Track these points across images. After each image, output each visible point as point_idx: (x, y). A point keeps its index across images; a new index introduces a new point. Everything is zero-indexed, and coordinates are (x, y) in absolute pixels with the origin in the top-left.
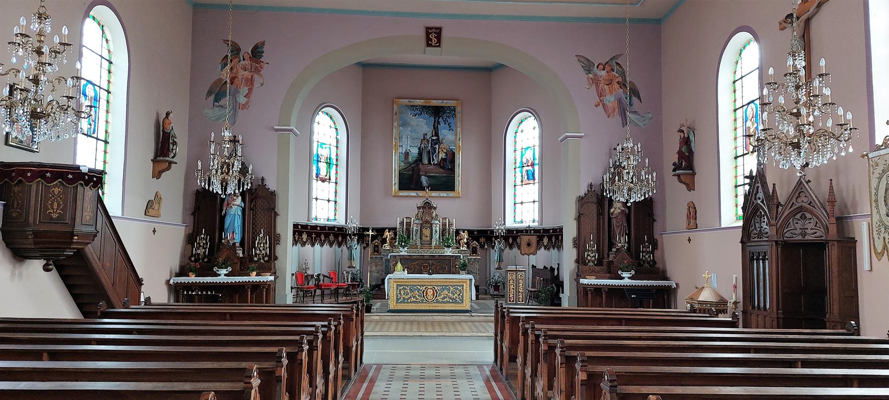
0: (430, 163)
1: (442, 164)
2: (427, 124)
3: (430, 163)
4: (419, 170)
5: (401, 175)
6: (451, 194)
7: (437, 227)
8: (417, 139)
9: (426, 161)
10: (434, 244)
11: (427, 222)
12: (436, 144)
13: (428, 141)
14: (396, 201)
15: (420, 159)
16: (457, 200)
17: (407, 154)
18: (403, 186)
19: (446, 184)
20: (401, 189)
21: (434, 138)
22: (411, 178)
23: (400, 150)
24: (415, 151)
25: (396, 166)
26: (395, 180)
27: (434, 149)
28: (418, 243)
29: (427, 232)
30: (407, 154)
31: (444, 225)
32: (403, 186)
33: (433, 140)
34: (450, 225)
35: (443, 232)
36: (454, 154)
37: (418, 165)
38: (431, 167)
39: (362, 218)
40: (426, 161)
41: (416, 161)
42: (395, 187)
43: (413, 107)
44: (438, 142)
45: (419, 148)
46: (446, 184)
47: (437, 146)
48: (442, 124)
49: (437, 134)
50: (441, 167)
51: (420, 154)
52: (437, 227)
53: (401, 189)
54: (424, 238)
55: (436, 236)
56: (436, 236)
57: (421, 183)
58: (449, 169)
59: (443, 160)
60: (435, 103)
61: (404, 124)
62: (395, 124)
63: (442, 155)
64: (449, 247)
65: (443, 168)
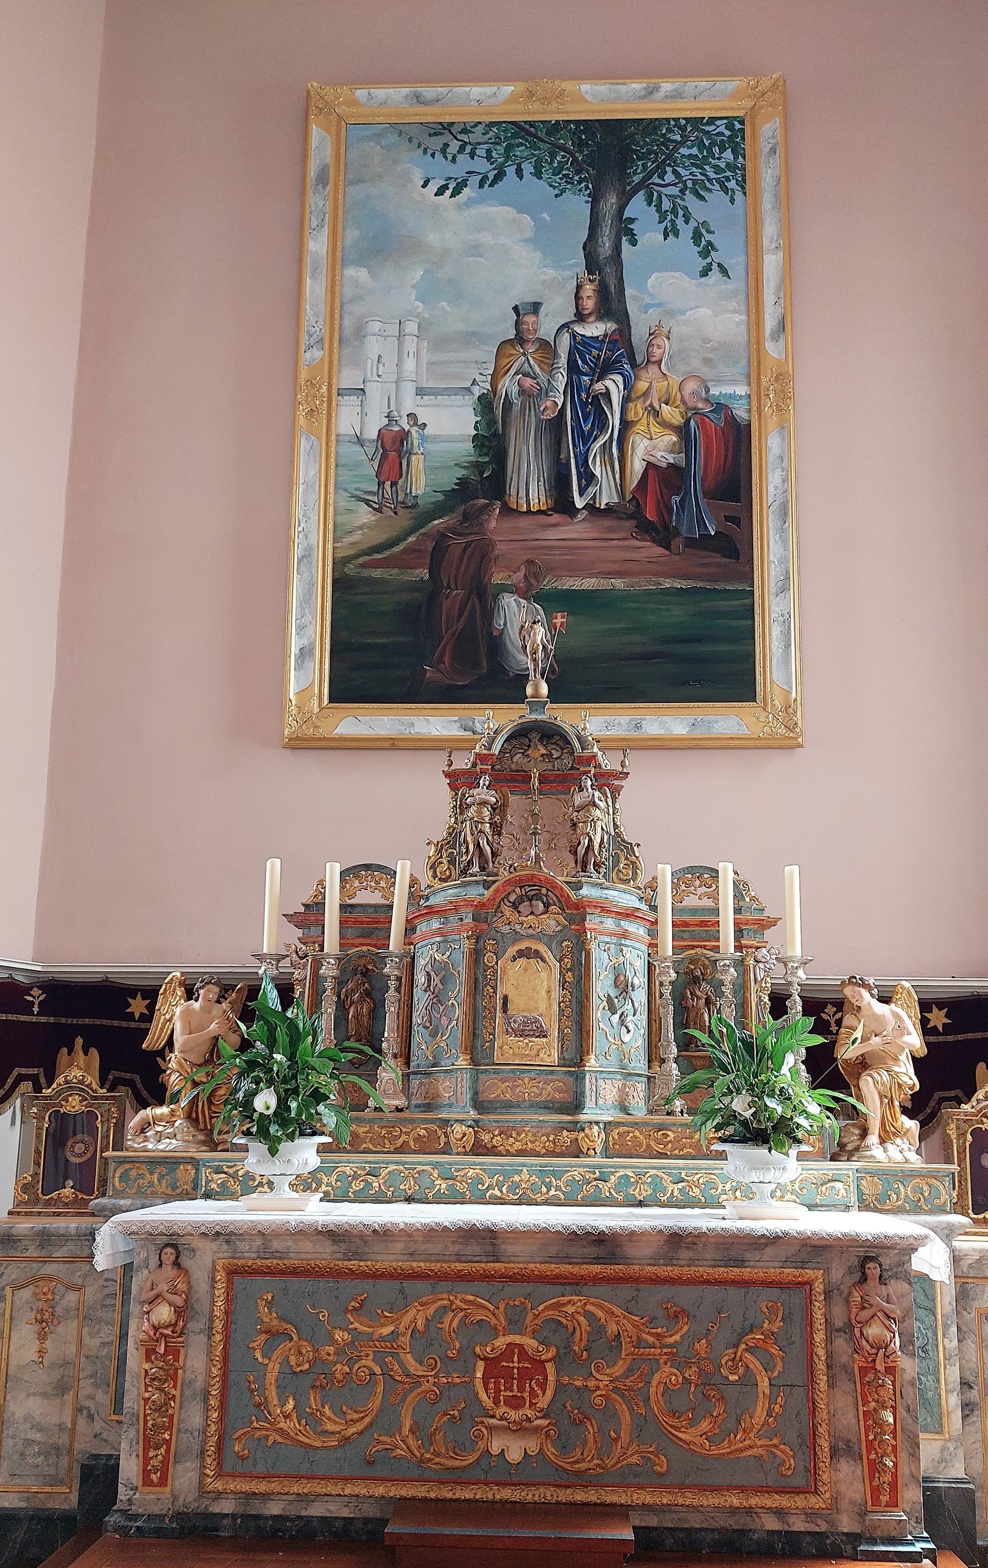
0: (562, 504)
1: (654, 508)
2: (540, 240)
3: (562, 504)
4: (482, 555)
5: (350, 591)
6: (725, 720)
7: (625, 956)
8: (470, 338)
9: (529, 486)
10: (600, 1107)
11: (532, 891)
12: (605, 369)
13: (547, 349)
14: (317, 779)
15: (486, 478)
16: (777, 763)
17: (394, 448)
18: (363, 672)
19: (699, 649)
20: (349, 687)
21: (594, 329)
22: (420, 612)
23: (348, 419)
24: (450, 427)
25: (315, 525)
26: (307, 626)
27: (595, 409)
28: (455, 1089)
29: (532, 987)
30: (394, 448)
31: (696, 928)
32: (363, 672)
33: (580, 346)
34: (754, 924)
35: (688, 994)
36: (737, 440)
37: (472, 519)
38: (575, 531)
39: (49, 917)
40: (530, 489)
41: (463, 490)
42: (306, 675)
43: (445, 136)
44: (619, 354)
45: (485, 404)
46: (699, 649)
47: (614, 385)
48: (650, 234)
49: (611, 303)
50: (645, 529)
51: (492, 443)
52: (625, 956)
53: (349, 687)
54: (508, 1048)
55: (620, 1037)
56: (620, 1037)
57: (496, 645)
58: (704, 543)
59: (665, 478)
60: (597, 99)
61: (383, 246)
62: (318, 245)
63: (652, 446)
64: (764, 1133)
65: (661, 533)
